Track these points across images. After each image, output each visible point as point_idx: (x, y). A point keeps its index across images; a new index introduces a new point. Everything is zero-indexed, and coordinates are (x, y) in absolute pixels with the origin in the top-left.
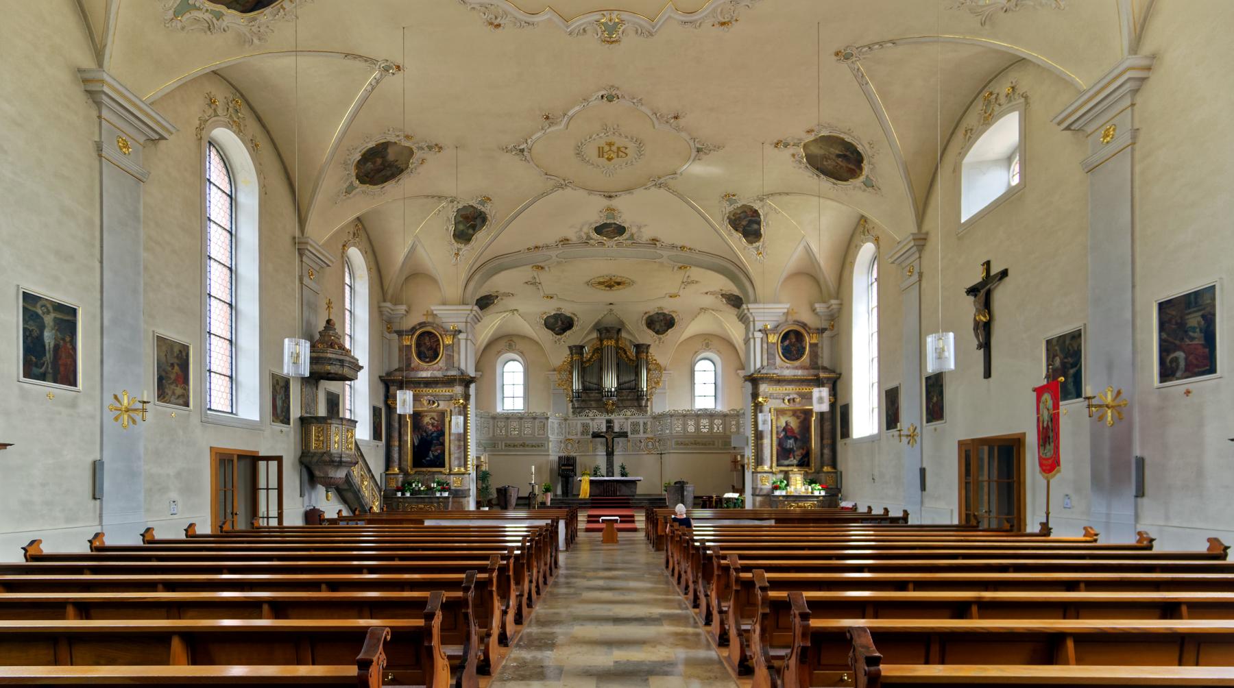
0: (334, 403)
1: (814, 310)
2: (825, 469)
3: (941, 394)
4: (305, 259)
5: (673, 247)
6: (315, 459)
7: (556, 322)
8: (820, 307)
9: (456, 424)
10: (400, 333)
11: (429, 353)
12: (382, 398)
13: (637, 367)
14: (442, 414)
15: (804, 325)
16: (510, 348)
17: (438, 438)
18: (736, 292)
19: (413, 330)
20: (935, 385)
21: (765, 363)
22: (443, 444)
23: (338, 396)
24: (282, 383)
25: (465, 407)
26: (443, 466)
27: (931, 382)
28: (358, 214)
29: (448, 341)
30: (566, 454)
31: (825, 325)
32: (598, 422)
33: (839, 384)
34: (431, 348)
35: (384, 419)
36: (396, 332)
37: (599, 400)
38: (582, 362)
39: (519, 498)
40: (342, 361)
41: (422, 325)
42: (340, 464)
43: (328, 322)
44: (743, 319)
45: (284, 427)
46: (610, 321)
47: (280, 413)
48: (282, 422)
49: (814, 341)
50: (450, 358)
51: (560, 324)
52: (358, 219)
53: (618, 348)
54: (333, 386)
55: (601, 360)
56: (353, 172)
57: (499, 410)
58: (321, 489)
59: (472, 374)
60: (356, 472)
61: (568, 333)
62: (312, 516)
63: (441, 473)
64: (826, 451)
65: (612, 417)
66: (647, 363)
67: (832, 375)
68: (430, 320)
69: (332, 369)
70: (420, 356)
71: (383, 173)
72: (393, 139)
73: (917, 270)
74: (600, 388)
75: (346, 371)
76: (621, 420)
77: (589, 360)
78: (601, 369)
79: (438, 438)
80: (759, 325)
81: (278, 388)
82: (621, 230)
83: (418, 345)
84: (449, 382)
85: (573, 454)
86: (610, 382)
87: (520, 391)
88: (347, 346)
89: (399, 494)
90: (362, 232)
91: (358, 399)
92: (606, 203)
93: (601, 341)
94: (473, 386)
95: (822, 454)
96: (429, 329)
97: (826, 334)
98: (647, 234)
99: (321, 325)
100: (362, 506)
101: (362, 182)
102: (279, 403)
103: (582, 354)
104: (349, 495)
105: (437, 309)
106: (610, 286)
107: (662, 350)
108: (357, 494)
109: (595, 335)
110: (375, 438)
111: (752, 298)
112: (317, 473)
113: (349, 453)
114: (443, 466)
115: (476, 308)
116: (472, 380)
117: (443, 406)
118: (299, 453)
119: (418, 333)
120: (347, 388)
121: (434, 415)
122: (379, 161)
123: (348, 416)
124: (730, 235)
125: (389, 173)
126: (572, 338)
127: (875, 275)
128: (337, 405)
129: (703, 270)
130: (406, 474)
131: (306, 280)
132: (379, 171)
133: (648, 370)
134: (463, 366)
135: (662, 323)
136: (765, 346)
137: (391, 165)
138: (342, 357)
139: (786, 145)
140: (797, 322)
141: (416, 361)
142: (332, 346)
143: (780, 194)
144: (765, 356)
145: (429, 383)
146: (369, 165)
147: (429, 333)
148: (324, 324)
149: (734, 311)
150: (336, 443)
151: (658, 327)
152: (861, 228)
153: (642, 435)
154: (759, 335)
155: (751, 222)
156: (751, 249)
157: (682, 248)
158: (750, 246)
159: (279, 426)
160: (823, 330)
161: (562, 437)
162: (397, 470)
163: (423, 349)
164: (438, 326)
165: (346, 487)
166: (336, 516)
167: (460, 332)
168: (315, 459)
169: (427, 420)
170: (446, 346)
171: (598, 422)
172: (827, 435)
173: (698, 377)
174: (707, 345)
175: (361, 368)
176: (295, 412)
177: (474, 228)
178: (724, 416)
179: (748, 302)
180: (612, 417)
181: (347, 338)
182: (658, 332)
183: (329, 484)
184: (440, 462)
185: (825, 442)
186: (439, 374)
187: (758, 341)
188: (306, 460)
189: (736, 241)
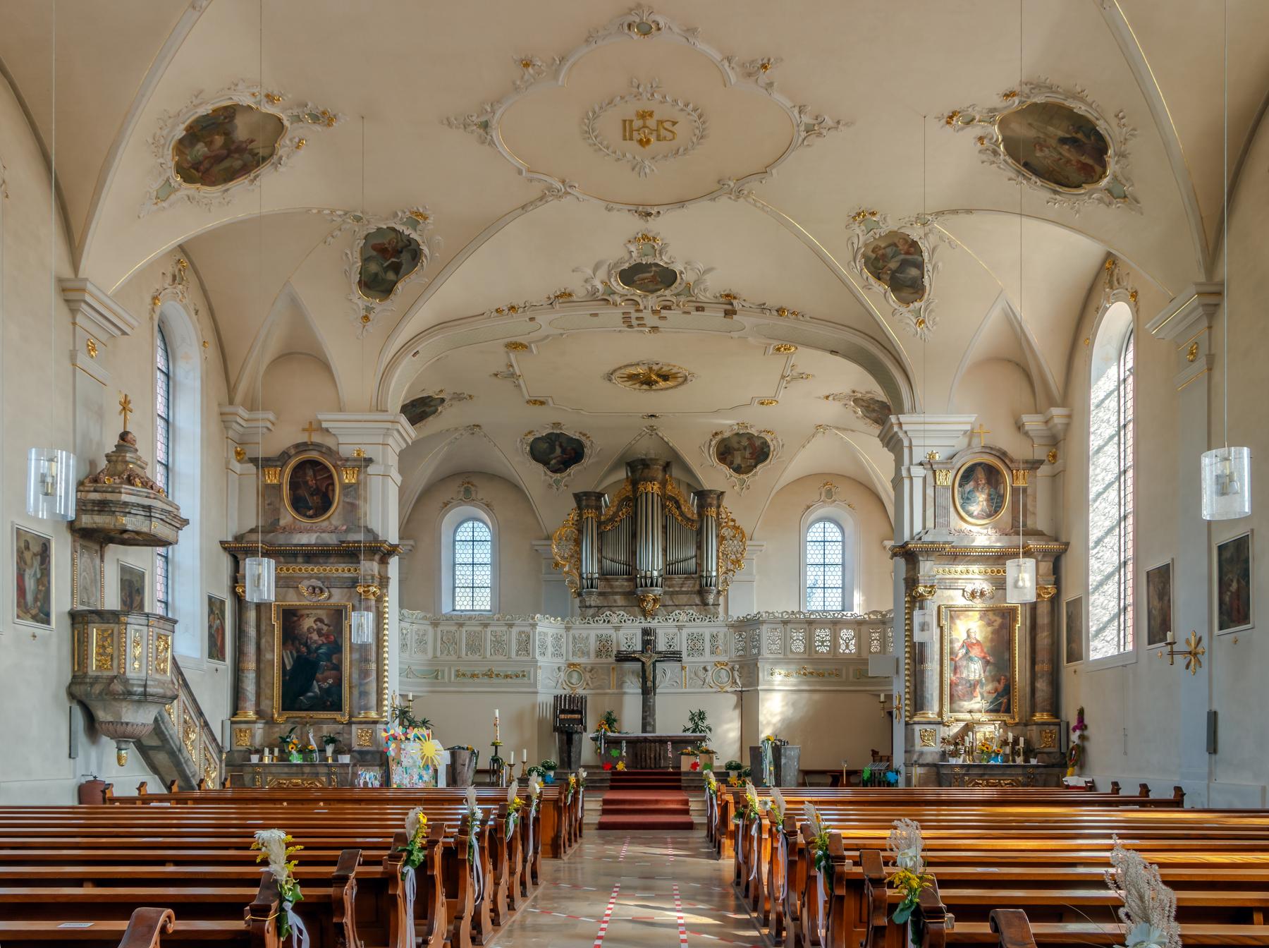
0: (132, 588)
1: (1019, 427)
2: (1038, 717)
3: (1245, 575)
4: (80, 319)
5: (762, 308)
6: (97, 689)
7: (552, 449)
8: (1032, 422)
9: (361, 626)
10: (263, 463)
12: (226, 581)
13: (699, 532)
15: (1002, 455)
16: (468, 496)
17: (329, 656)
18: (880, 394)
19: (284, 457)
20: (1234, 560)
21: (930, 524)
22: (338, 668)
23: (142, 576)
24: (35, 548)
25: (380, 600)
26: (337, 707)
27: (1227, 555)
28: (180, 239)
29: (349, 478)
30: (568, 691)
31: (1040, 453)
32: (626, 631)
33: (1067, 563)
34: (317, 491)
35: (230, 623)
36: (254, 461)
37: (629, 594)
38: (600, 524)
39: (478, 772)
40: (149, 508)
41: (301, 447)
42: (145, 698)
43: (124, 436)
44: (892, 442)
45: (39, 629)
46: (646, 447)
47: (34, 605)
48: (35, 618)
49: (1020, 483)
50: (352, 508)
51: (559, 452)
52: (181, 248)
53: (665, 497)
54: (136, 557)
55: (634, 519)
56: (169, 159)
57: (446, 609)
58: (109, 745)
59: (393, 538)
60: (175, 715)
61: (574, 469)
62: (91, 791)
63: (335, 721)
64: (1042, 685)
65: (653, 624)
66: (719, 525)
67: (1054, 546)
68: (316, 438)
69: (132, 522)
70: (299, 504)
71: (226, 164)
72: (246, 100)
73: (1204, 350)
74: (631, 572)
75: (158, 529)
76: (667, 631)
77: (612, 520)
78: (634, 536)
79: (329, 656)
80: (919, 455)
81: (28, 555)
82: (667, 277)
83: (294, 485)
84: (350, 553)
85: (580, 691)
86: (652, 561)
87: (484, 576)
88: (160, 481)
89: (255, 759)
90: (189, 275)
91: (185, 579)
92: (636, 225)
93: (634, 483)
94: (394, 562)
95: (1033, 690)
96: (314, 455)
97: (1044, 470)
98: (714, 285)
99: (110, 444)
100: (186, 779)
101: (188, 179)
102: (30, 584)
103: (599, 508)
104: (161, 758)
105: (328, 419)
106: (649, 383)
107: (743, 500)
108: (175, 756)
109: (622, 474)
110: (211, 656)
111: (907, 404)
112: (102, 715)
113: (163, 680)
114: (337, 707)
115: (403, 419)
116: (392, 551)
117: (338, 597)
118: (68, 678)
119: (293, 463)
120: (160, 562)
121: (322, 614)
122: (219, 140)
123: (160, 610)
124: (867, 287)
125: (237, 164)
126: (580, 477)
127: (1130, 364)
128: (140, 591)
129: (819, 353)
130: (270, 722)
131: (82, 359)
132: (218, 159)
133: (721, 539)
134: (375, 524)
135: (745, 452)
136: (930, 491)
137: (240, 149)
138: (147, 502)
139: (969, 122)
140: (989, 450)
141: (288, 516)
142: (130, 481)
143: (955, 212)
144: (930, 512)
145: (312, 555)
146: (201, 149)
147: (314, 463)
148: (116, 440)
149: (876, 430)
150: (137, 657)
151: (738, 460)
152: (1105, 277)
153: (707, 656)
154: (918, 472)
155: (904, 264)
156: (907, 314)
157: (780, 311)
158: (903, 309)
159: (29, 627)
160: (1034, 465)
161: (561, 661)
162: (251, 715)
163: (303, 492)
164: (330, 452)
165: (155, 742)
166: (136, 793)
168: (97, 689)
169: (308, 623)
170: (346, 487)
171: (626, 631)
172: (1043, 655)
173: (813, 554)
174: (829, 494)
175: (186, 522)
176: (61, 602)
177: (396, 268)
178: (858, 624)
179: (900, 411)
180: (653, 624)
181: (160, 469)
182: (738, 470)
183: (122, 736)
185: (1037, 668)
186: (331, 539)
187: (918, 484)
188: (78, 690)
189: (878, 300)
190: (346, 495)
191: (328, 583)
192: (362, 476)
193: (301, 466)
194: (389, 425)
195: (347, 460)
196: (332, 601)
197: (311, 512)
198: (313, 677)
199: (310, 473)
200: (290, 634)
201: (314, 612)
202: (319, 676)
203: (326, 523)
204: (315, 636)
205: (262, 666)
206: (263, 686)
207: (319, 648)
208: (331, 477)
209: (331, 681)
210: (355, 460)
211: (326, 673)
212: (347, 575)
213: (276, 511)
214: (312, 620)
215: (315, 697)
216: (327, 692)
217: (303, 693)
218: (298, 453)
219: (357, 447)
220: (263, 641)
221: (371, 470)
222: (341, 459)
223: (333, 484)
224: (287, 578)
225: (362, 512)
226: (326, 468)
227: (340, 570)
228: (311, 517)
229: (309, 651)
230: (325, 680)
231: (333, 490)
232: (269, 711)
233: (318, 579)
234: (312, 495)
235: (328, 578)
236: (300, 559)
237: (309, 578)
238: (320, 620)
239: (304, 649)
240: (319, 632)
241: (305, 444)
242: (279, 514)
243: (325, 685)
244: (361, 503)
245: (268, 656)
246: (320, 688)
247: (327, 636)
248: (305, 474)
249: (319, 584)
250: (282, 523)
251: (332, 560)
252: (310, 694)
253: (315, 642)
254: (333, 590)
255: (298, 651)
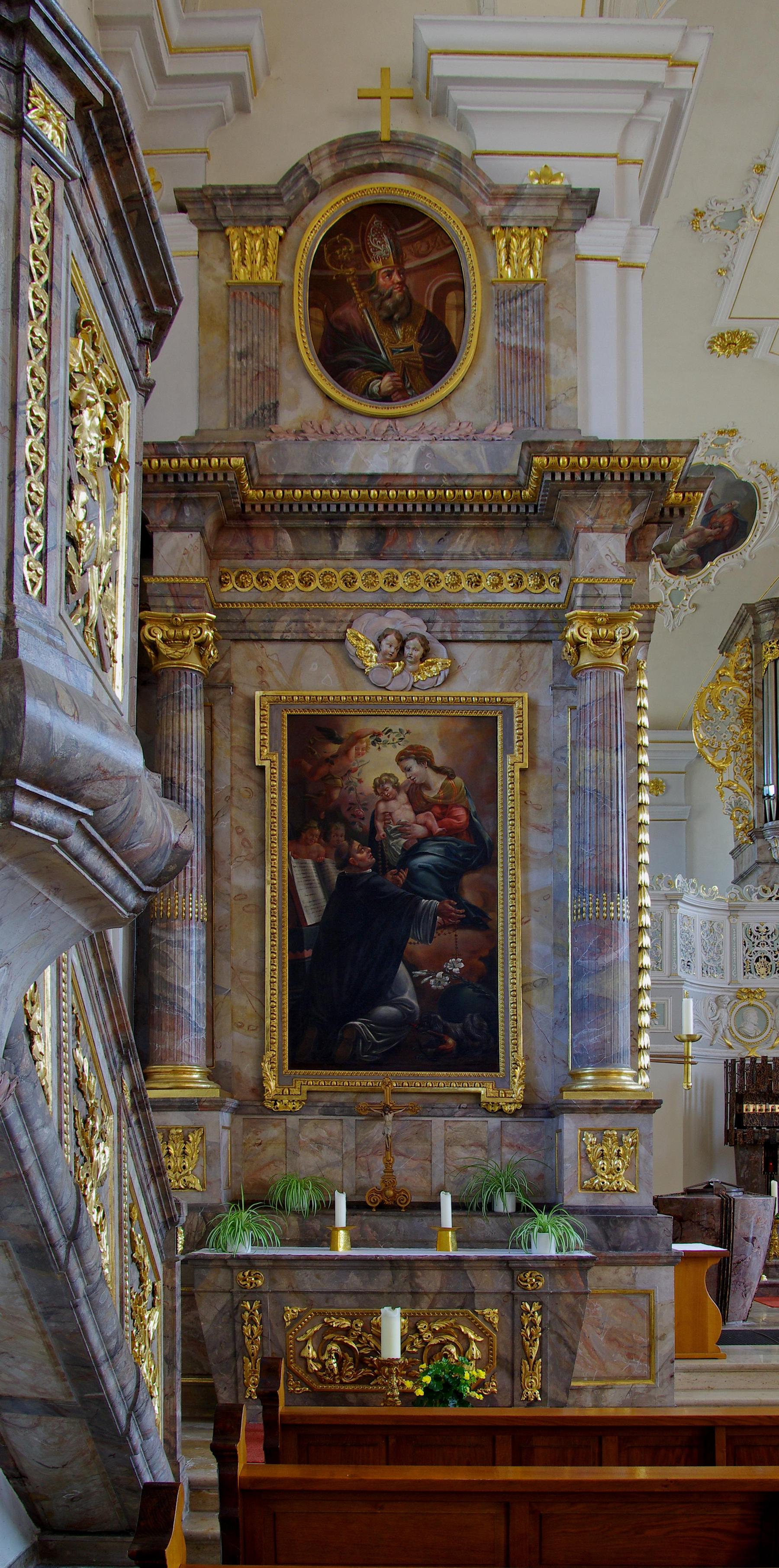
11: (399, 342)
14: (482, 730)
17: (449, 879)
22: (481, 919)
41: (357, 154)
50: (527, 367)
68: (404, 124)
70: (343, 355)
79: (449, 879)
83: (324, 288)
96: (394, 186)
119: (324, 214)
121: (426, 732)
130: (252, 1105)
141: (305, 393)
145: (391, 521)
147: (397, 215)
162: (195, 1080)
163: (359, 314)
167: (585, 203)
169: (376, 764)
184: (461, 1033)
190: (505, 324)
191: (446, 628)
192: (557, 262)
193: (353, 225)
194: (656, 72)
195: (514, 196)
196: (459, 689)
197: (386, 383)
198: (396, 952)
199: (382, 247)
200: (317, 799)
201: (396, 725)
202: (416, 947)
203: (437, 419)
204: (402, 810)
205: (221, 912)
206: (224, 980)
207: (413, 851)
208: (453, 260)
209: (457, 966)
210: (542, 197)
211: (444, 938)
212: (510, 597)
213: (267, 377)
214: (391, 752)
215: (405, 1020)
216: (446, 1002)
217: (364, 1008)
218: (341, 179)
219: (539, 163)
220: (223, 825)
221: (591, 238)
222: (494, 194)
223: (461, 286)
224: (303, 608)
225: (557, 382)
226: (434, 231)
227: (488, 578)
228: (385, 398)
229: (382, 864)
230: (437, 961)
231: (462, 308)
232: (247, 1069)
233: (414, 611)
234: (389, 321)
235: (447, 608)
236: (349, 543)
237: (382, 608)
238: (422, 756)
239: (364, 855)
240: (415, 793)
241: (369, 141)
242: (274, 388)
243: (439, 981)
244: (555, 351)
245: (242, 879)
246: (421, 990)
247: (444, 809)
248: (364, 253)
249: (417, 625)
250: (287, 418)
251: (460, 544)
252: (386, 1011)
253: (403, 829)
254: (462, 651)
255: (344, 860)
